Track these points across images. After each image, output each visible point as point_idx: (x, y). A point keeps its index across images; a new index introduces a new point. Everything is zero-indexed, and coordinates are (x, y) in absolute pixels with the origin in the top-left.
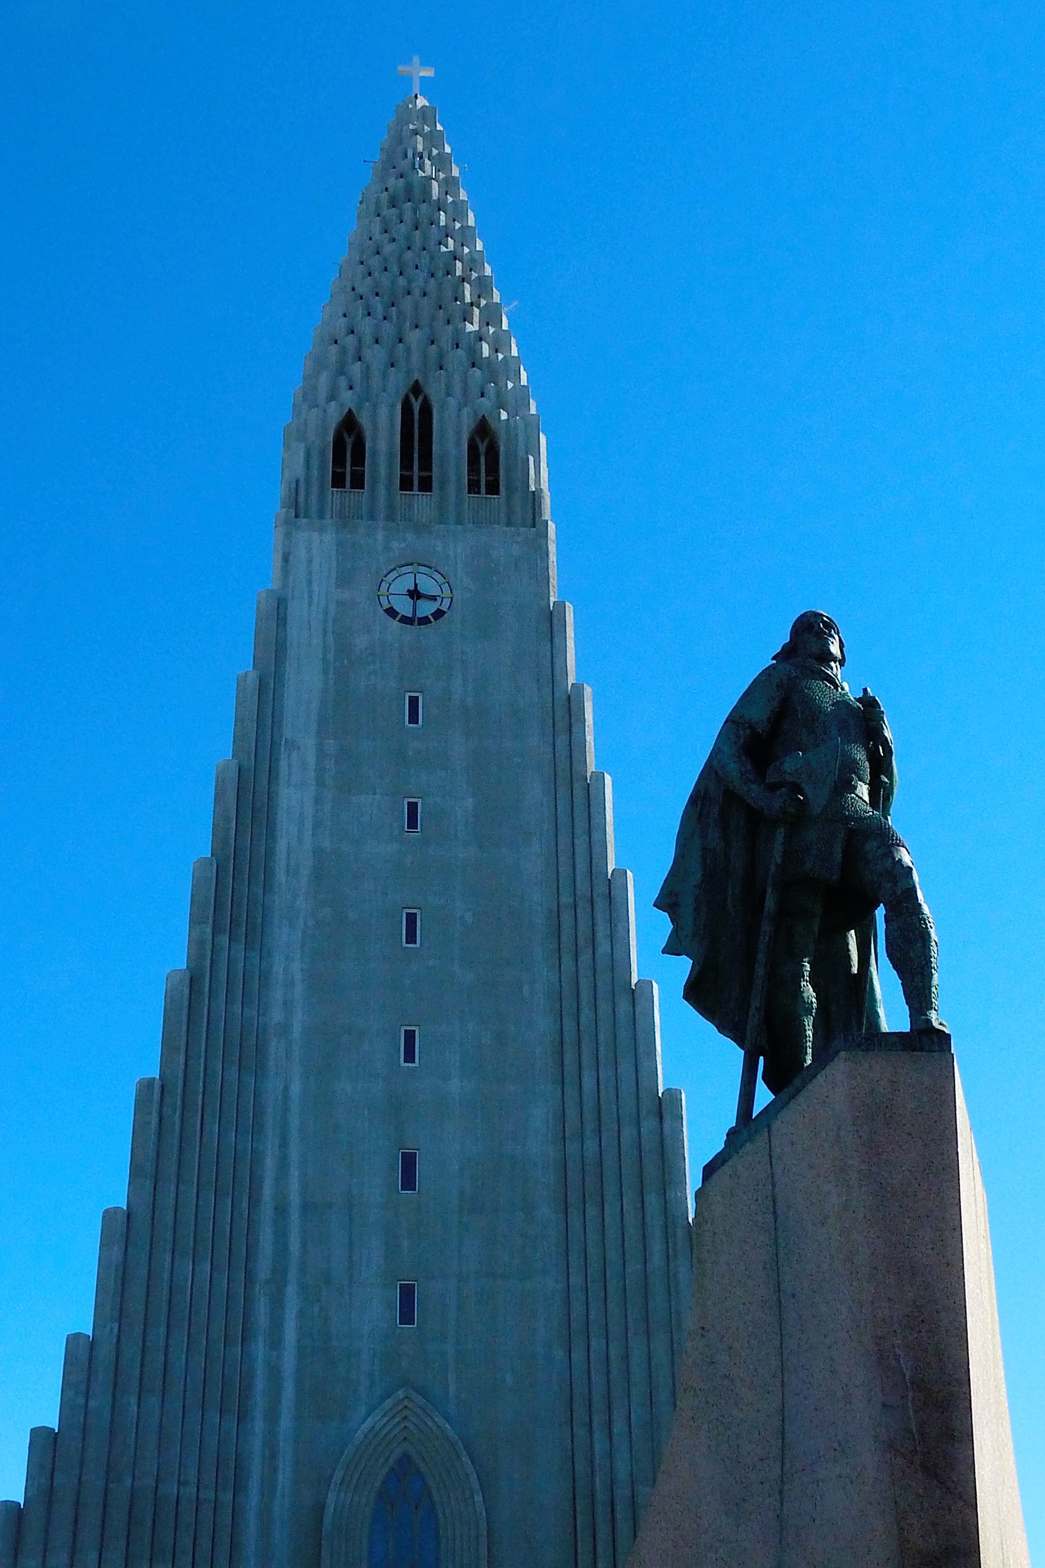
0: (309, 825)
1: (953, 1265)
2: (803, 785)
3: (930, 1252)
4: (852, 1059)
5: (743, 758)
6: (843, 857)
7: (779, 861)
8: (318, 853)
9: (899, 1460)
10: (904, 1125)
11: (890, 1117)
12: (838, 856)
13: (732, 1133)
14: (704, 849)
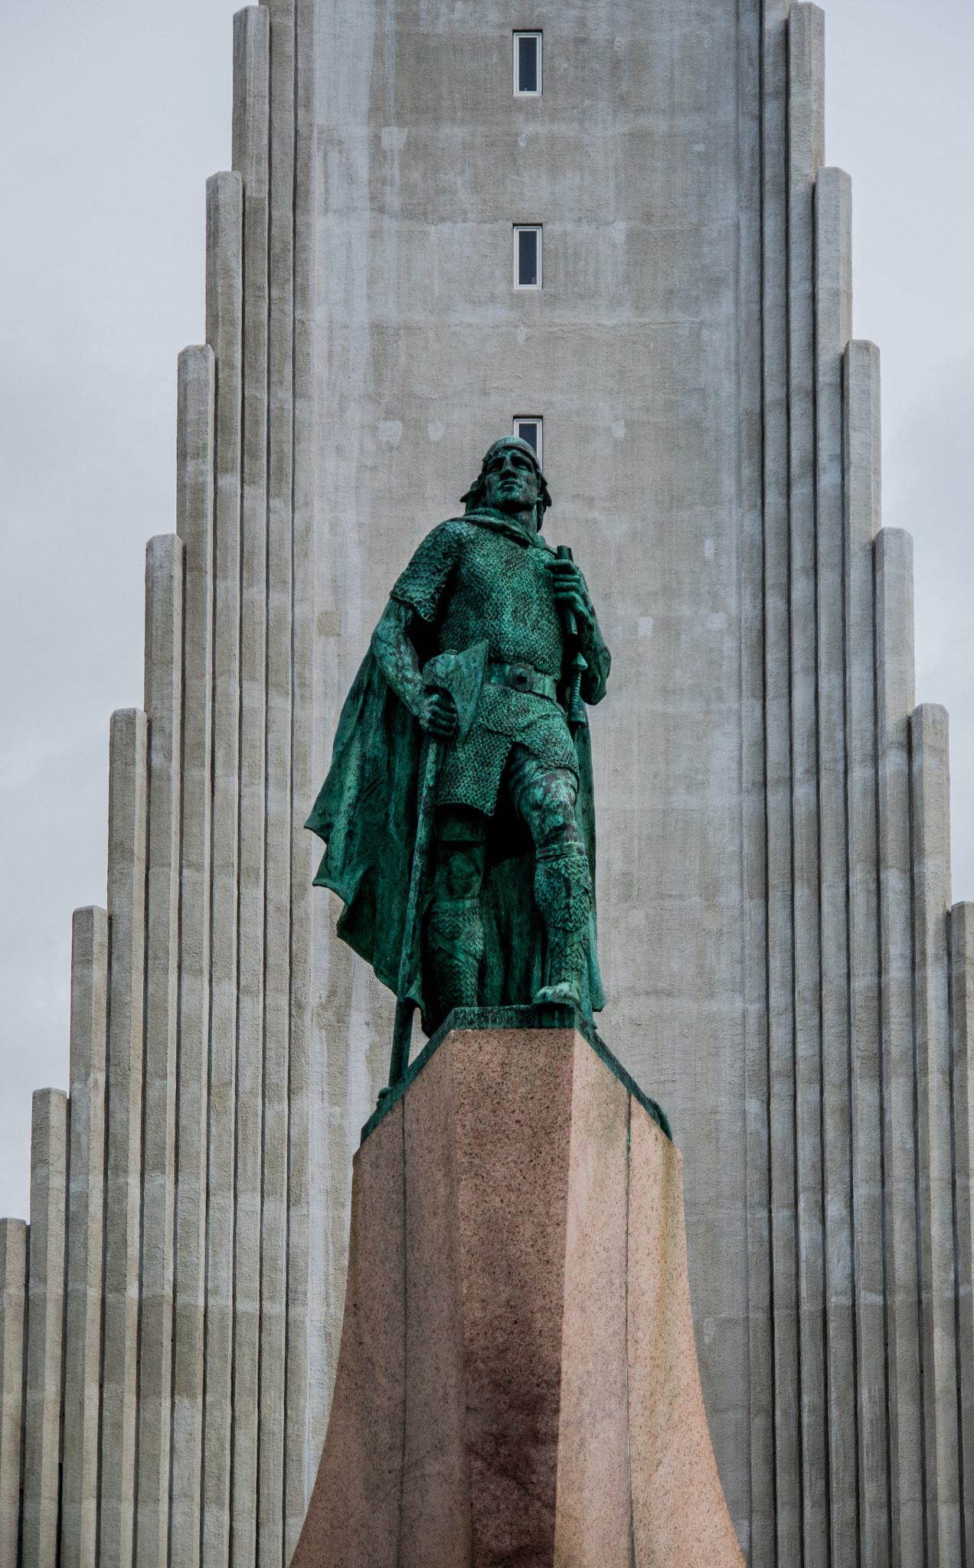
0: (361, 278)
1: (553, 1263)
2: (454, 695)
3: (530, 1250)
4: (461, 1040)
5: (403, 648)
6: (501, 780)
7: (431, 784)
8: (378, 329)
9: (478, 1464)
10: (513, 1112)
11: (498, 1103)
12: (497, 778)
13: (383, 1095)
14: (363, 755)
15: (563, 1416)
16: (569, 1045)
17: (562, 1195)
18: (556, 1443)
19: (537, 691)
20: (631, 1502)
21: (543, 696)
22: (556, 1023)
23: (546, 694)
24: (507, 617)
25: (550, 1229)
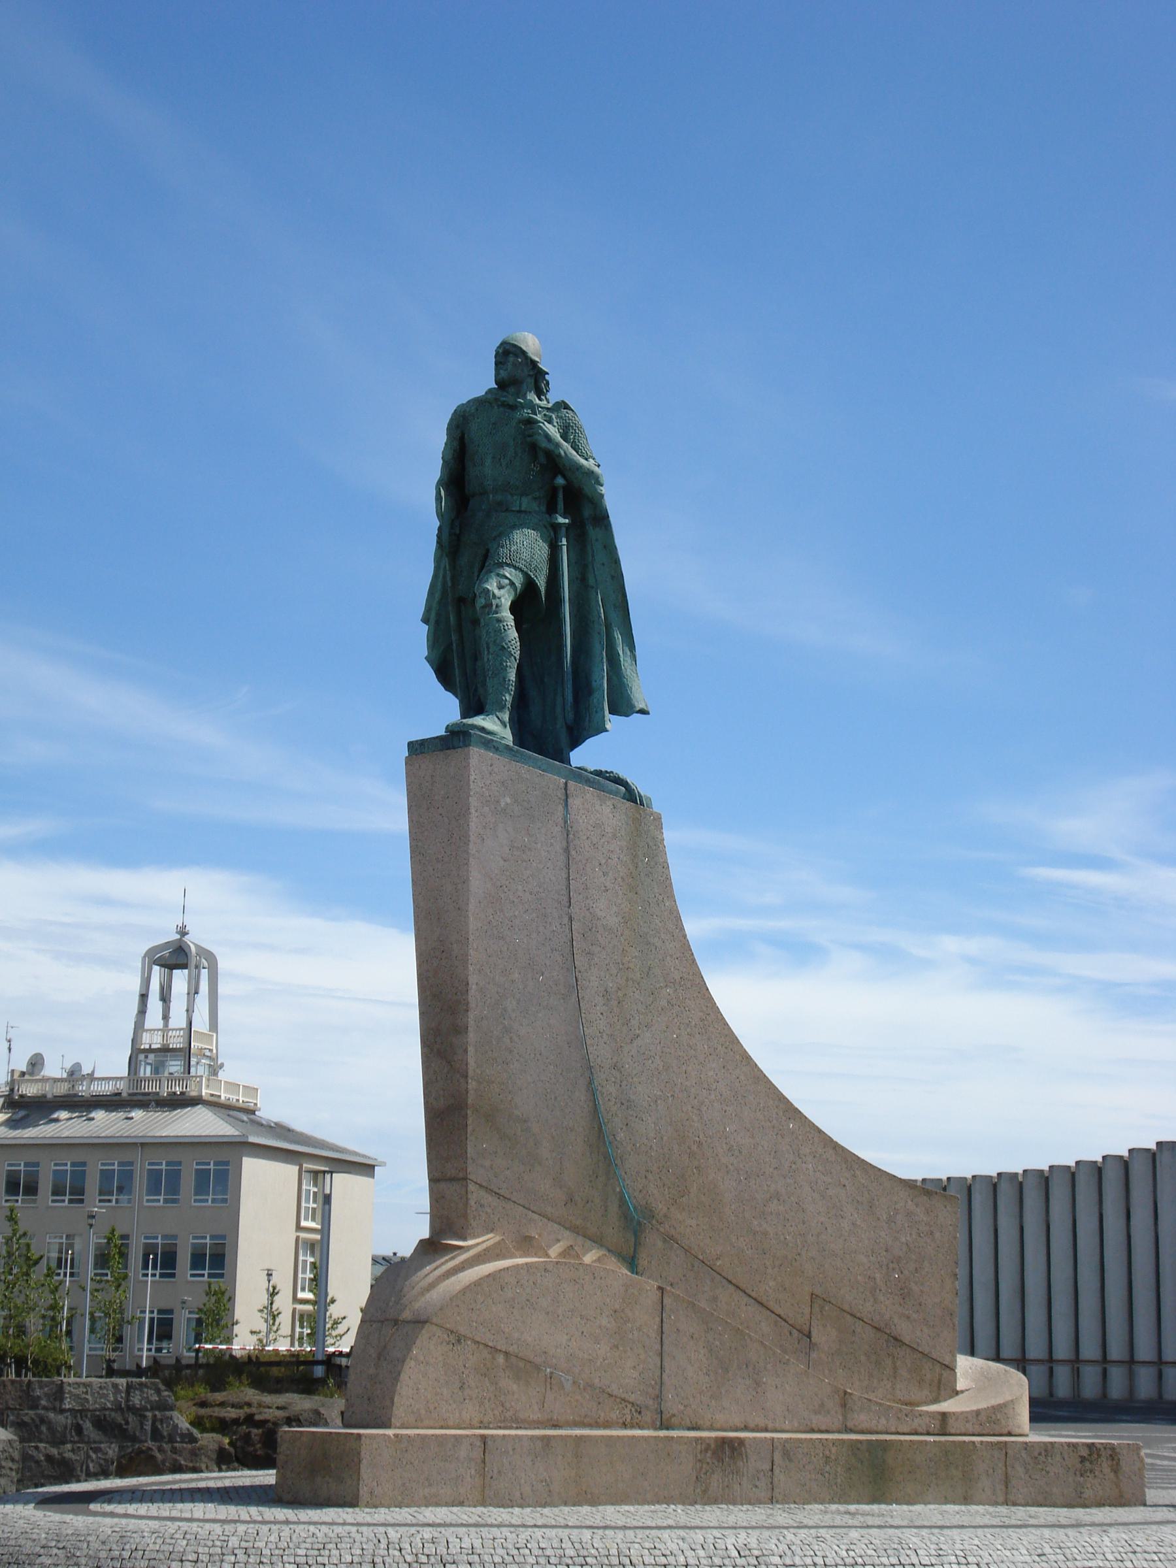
15: (472, 1016)
16: (467, 757)
17: (465, 862)
18: (467, 1033)
19: (514, 509)
20: (591, 1068)
21: (520, 512)
22: (461, 744)
23: (523, 509)
24: (488, 462)
25: (459, 886)
